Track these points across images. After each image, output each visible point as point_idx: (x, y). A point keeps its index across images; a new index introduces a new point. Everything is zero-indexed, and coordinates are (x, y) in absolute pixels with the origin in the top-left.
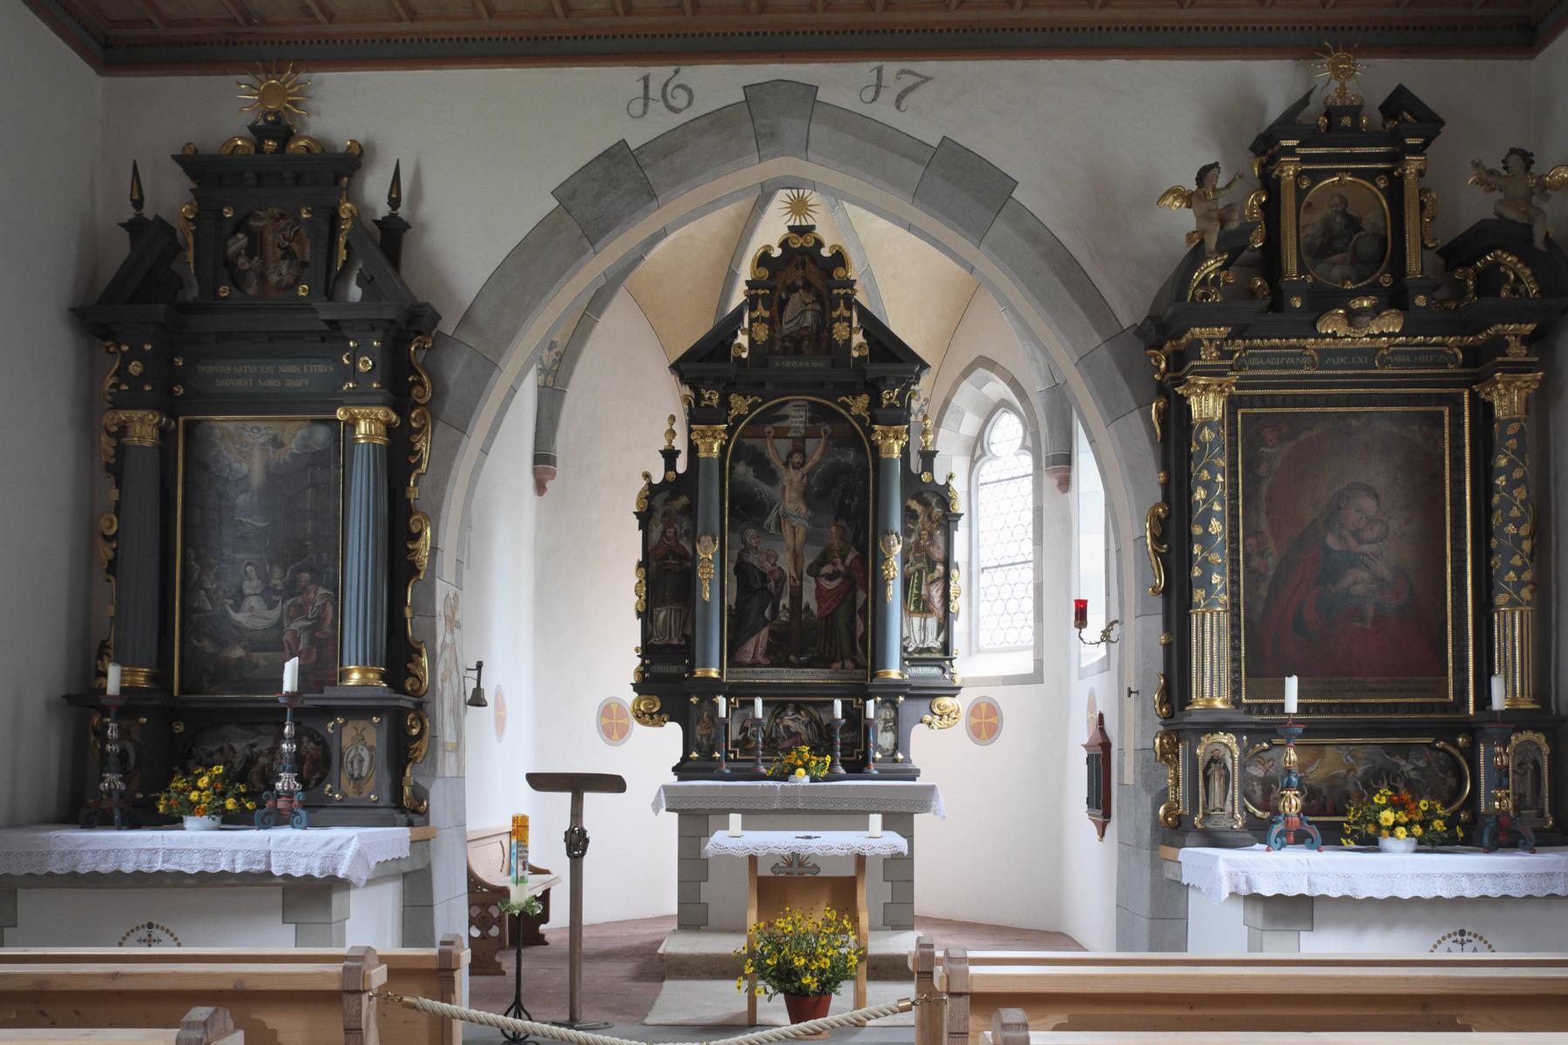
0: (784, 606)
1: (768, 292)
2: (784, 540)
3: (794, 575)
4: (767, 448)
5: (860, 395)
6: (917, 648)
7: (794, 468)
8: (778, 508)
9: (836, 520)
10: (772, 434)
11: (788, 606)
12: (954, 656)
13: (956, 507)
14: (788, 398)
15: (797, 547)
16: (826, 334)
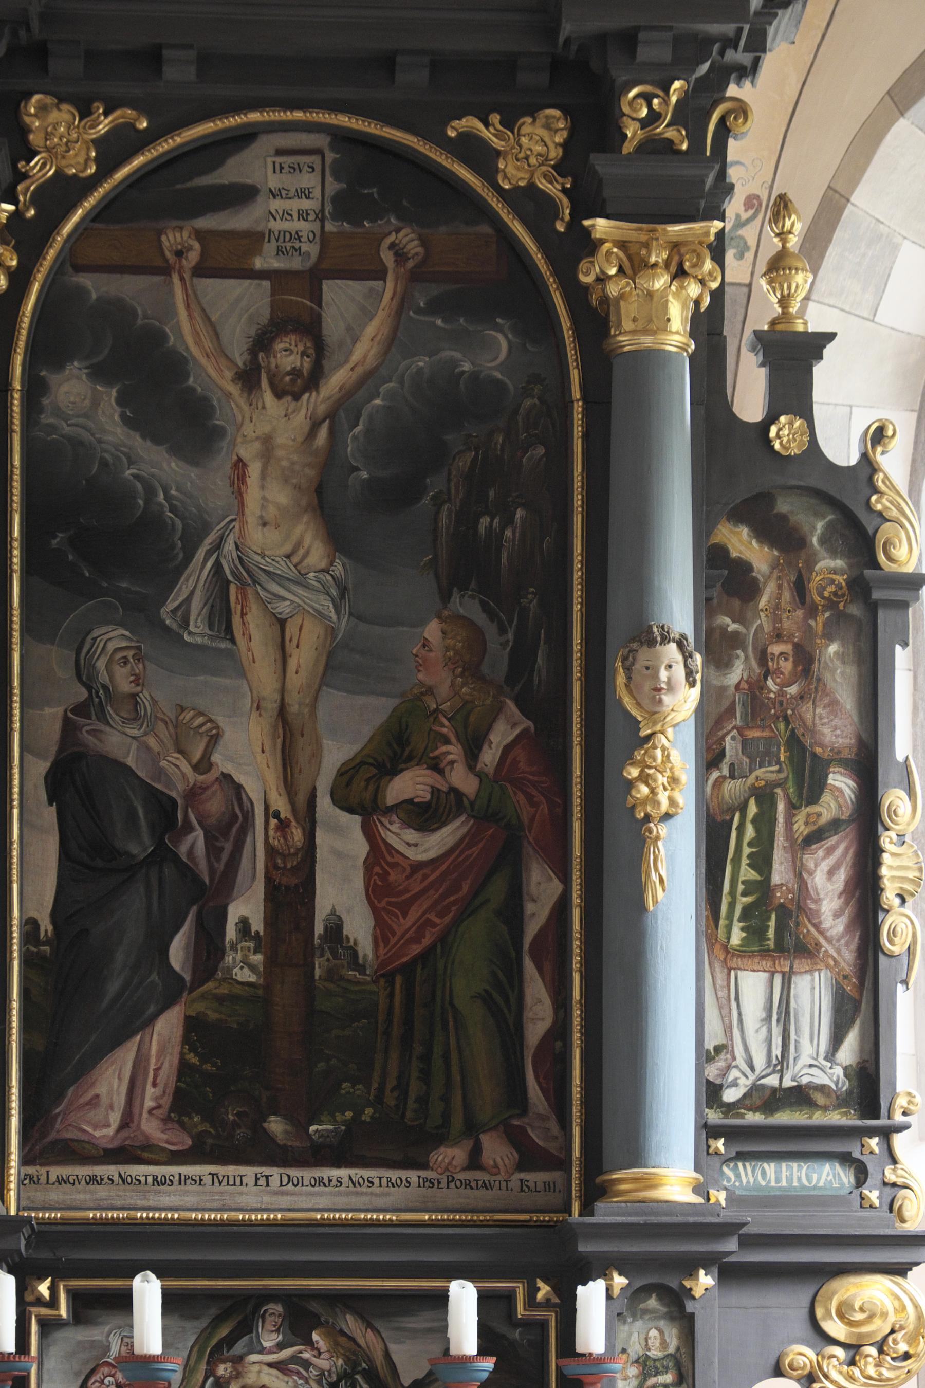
0: (244, 925)
2: (242, 673)
3: (280, 804)
4: (171, 311)
6: (755, 1088)
8: (218, 546)
9: (446, 597)
11: (257, 925)
12: (898, 1118)
13: (901, 552)
15: (294, 709)
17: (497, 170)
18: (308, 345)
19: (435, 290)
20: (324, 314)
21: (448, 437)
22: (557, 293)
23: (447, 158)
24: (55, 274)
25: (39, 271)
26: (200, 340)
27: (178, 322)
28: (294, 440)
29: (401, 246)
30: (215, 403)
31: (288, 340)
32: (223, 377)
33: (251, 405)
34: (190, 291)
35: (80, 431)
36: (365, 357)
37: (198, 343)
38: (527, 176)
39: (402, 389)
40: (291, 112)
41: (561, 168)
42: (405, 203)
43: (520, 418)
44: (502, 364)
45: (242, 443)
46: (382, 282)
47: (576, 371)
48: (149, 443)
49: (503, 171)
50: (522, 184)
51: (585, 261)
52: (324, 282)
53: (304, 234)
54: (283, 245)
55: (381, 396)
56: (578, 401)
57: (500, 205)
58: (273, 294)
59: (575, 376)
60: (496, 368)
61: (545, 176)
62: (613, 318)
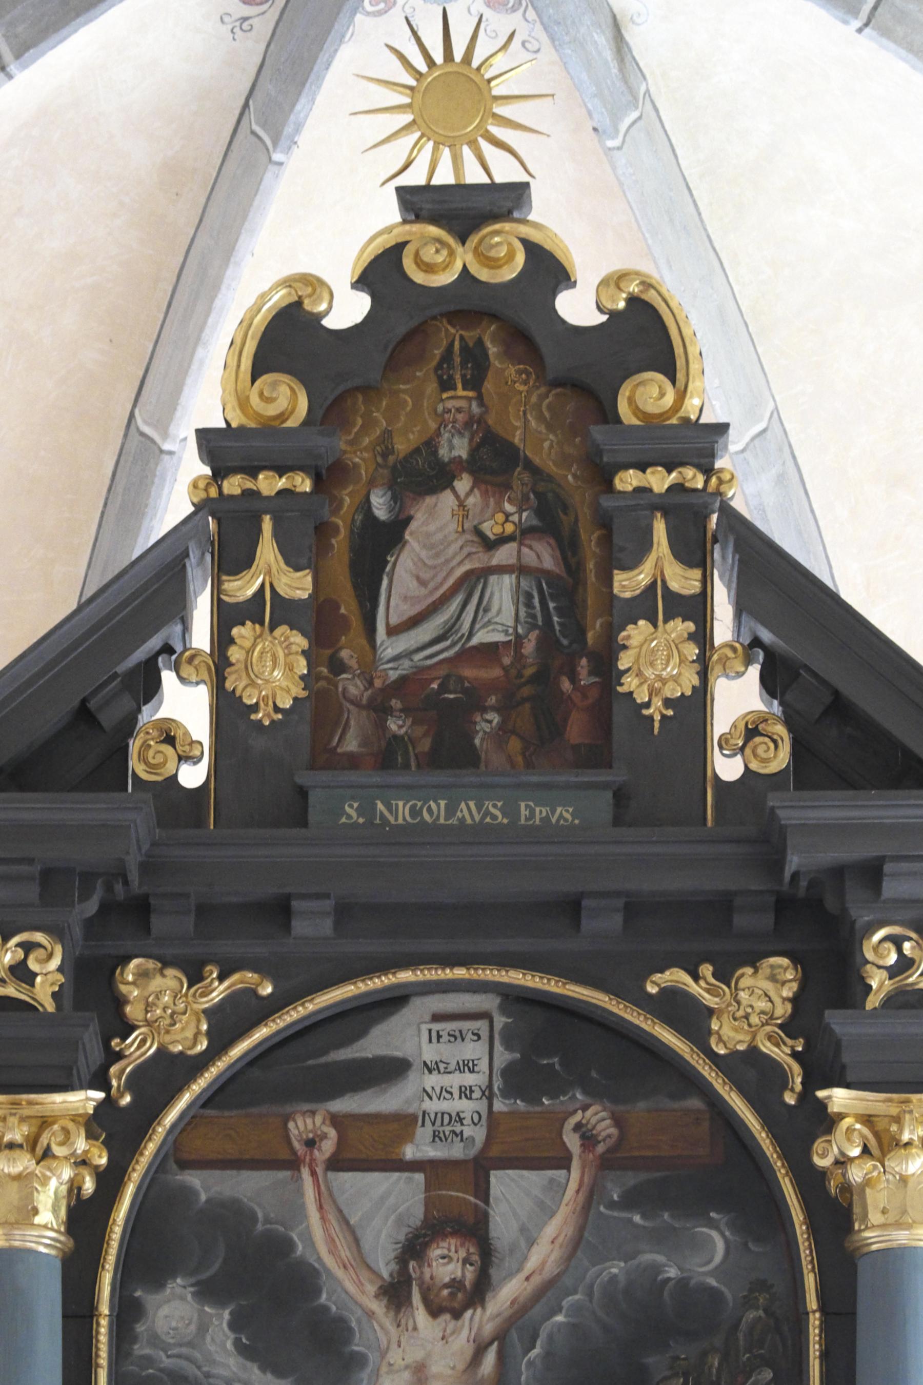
1: (303, 484)
5: (753, 960)
7: (434, 1311)
10: (328, 1147)
14: (405, 976)
16: (585, 679)
17: (709, 1032)
18: (472, 1250)
19: (631, 1179)
20: (491, 1212)
21: (650, 1360)
22: (787, 1180)
23: (646, 1019)
24: (156, 1172)
25: (134, 1170)
26: (336, 1247)
27: (308, 1227)
28: (453, 1368)
29: (589, 1127)
30: (353, 1324)
31: (445, 1244)
32: (363, 1292)
33: (399, 1326)
34: (323, 1187)
35: (183, 1363)
36: (544, 1263)
37: (333, 1251)
38: (748, 1038)
39: (591, 1301)
40: (451, 970)
41: (789, 1028)
42: (594, 1074)
43: (741, 1336)
44: (716, 1268)
45: (387, 1373)
46: (564, 1171)
47: (811, 1276)
48: (269, 1376)
49: (717, 1033)
50: (741, 1047)
51: (820, 1140)
52: (492, 1173)
53: (467, 1116)
54: (441, 1129)
55: (564, 1311)
56: (814, 1312)
57: (713, 1075)
58: (427, 1189)
59: (810, 1281)
60: (710, 1273)
61: (770, 1038)
62: (857, 1210)
